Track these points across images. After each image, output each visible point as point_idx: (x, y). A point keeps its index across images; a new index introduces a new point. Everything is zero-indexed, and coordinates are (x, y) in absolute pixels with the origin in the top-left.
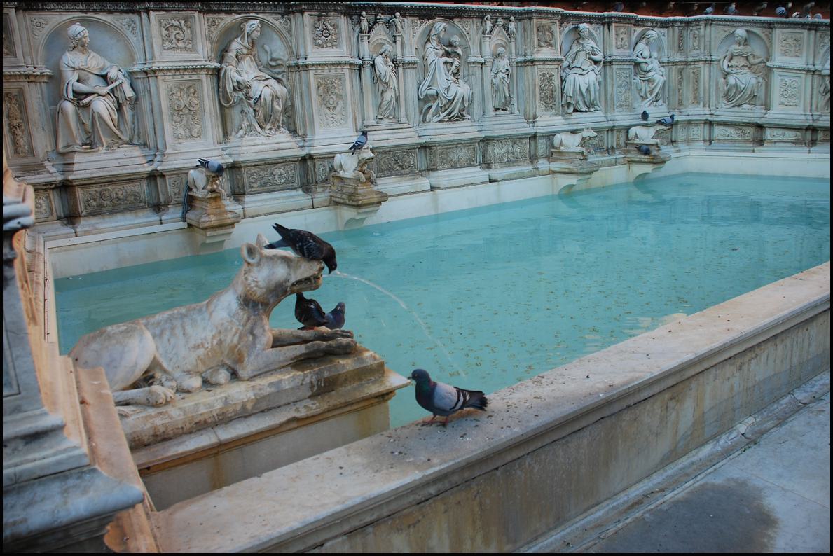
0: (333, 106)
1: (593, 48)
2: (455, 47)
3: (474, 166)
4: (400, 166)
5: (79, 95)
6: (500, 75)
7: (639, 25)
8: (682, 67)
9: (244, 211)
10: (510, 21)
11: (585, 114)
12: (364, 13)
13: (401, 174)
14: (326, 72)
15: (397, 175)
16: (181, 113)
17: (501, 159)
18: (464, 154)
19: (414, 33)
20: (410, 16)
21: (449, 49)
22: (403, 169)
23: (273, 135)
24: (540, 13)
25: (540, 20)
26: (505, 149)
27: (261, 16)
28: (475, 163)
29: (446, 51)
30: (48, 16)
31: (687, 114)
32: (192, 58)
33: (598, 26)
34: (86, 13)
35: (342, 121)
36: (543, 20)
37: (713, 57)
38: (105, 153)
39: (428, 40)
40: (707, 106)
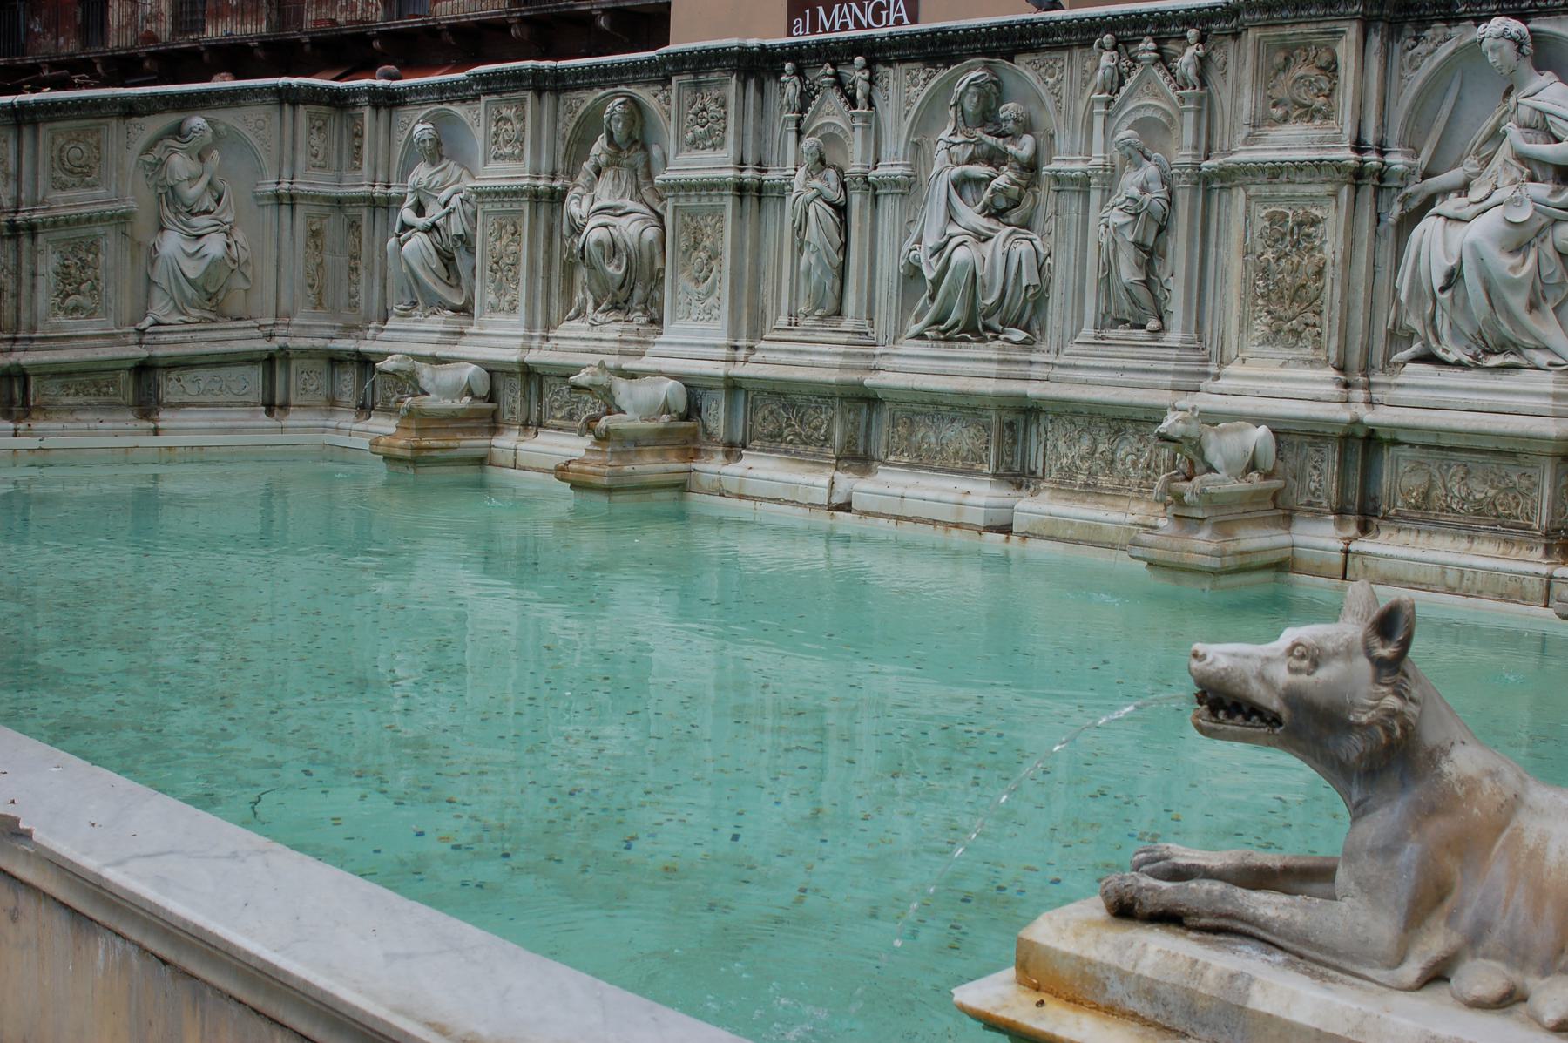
0: (702, 275)
1: (1542, 112)
3: (980, 474)
5: (405, 227)
9: (515, 454)
11: (1445, 371)
12: (788, 66)
13: (797, 453)
14: (694, 202)
15: (786, 453)
16: (495, 266)
17: (1068, 473)
18: (960, 437)
20: (902, 61)
22: (805, 443)
23: (602, 324)
25: (1271, 32)
26: (1085, 445)
27: (633, 90)
28: (986, 469)
30: (413, 112)
32: (516, 172)
34: (441, 103)
35: (715, 312)
36: (1288, 30)
38: (415, 321)
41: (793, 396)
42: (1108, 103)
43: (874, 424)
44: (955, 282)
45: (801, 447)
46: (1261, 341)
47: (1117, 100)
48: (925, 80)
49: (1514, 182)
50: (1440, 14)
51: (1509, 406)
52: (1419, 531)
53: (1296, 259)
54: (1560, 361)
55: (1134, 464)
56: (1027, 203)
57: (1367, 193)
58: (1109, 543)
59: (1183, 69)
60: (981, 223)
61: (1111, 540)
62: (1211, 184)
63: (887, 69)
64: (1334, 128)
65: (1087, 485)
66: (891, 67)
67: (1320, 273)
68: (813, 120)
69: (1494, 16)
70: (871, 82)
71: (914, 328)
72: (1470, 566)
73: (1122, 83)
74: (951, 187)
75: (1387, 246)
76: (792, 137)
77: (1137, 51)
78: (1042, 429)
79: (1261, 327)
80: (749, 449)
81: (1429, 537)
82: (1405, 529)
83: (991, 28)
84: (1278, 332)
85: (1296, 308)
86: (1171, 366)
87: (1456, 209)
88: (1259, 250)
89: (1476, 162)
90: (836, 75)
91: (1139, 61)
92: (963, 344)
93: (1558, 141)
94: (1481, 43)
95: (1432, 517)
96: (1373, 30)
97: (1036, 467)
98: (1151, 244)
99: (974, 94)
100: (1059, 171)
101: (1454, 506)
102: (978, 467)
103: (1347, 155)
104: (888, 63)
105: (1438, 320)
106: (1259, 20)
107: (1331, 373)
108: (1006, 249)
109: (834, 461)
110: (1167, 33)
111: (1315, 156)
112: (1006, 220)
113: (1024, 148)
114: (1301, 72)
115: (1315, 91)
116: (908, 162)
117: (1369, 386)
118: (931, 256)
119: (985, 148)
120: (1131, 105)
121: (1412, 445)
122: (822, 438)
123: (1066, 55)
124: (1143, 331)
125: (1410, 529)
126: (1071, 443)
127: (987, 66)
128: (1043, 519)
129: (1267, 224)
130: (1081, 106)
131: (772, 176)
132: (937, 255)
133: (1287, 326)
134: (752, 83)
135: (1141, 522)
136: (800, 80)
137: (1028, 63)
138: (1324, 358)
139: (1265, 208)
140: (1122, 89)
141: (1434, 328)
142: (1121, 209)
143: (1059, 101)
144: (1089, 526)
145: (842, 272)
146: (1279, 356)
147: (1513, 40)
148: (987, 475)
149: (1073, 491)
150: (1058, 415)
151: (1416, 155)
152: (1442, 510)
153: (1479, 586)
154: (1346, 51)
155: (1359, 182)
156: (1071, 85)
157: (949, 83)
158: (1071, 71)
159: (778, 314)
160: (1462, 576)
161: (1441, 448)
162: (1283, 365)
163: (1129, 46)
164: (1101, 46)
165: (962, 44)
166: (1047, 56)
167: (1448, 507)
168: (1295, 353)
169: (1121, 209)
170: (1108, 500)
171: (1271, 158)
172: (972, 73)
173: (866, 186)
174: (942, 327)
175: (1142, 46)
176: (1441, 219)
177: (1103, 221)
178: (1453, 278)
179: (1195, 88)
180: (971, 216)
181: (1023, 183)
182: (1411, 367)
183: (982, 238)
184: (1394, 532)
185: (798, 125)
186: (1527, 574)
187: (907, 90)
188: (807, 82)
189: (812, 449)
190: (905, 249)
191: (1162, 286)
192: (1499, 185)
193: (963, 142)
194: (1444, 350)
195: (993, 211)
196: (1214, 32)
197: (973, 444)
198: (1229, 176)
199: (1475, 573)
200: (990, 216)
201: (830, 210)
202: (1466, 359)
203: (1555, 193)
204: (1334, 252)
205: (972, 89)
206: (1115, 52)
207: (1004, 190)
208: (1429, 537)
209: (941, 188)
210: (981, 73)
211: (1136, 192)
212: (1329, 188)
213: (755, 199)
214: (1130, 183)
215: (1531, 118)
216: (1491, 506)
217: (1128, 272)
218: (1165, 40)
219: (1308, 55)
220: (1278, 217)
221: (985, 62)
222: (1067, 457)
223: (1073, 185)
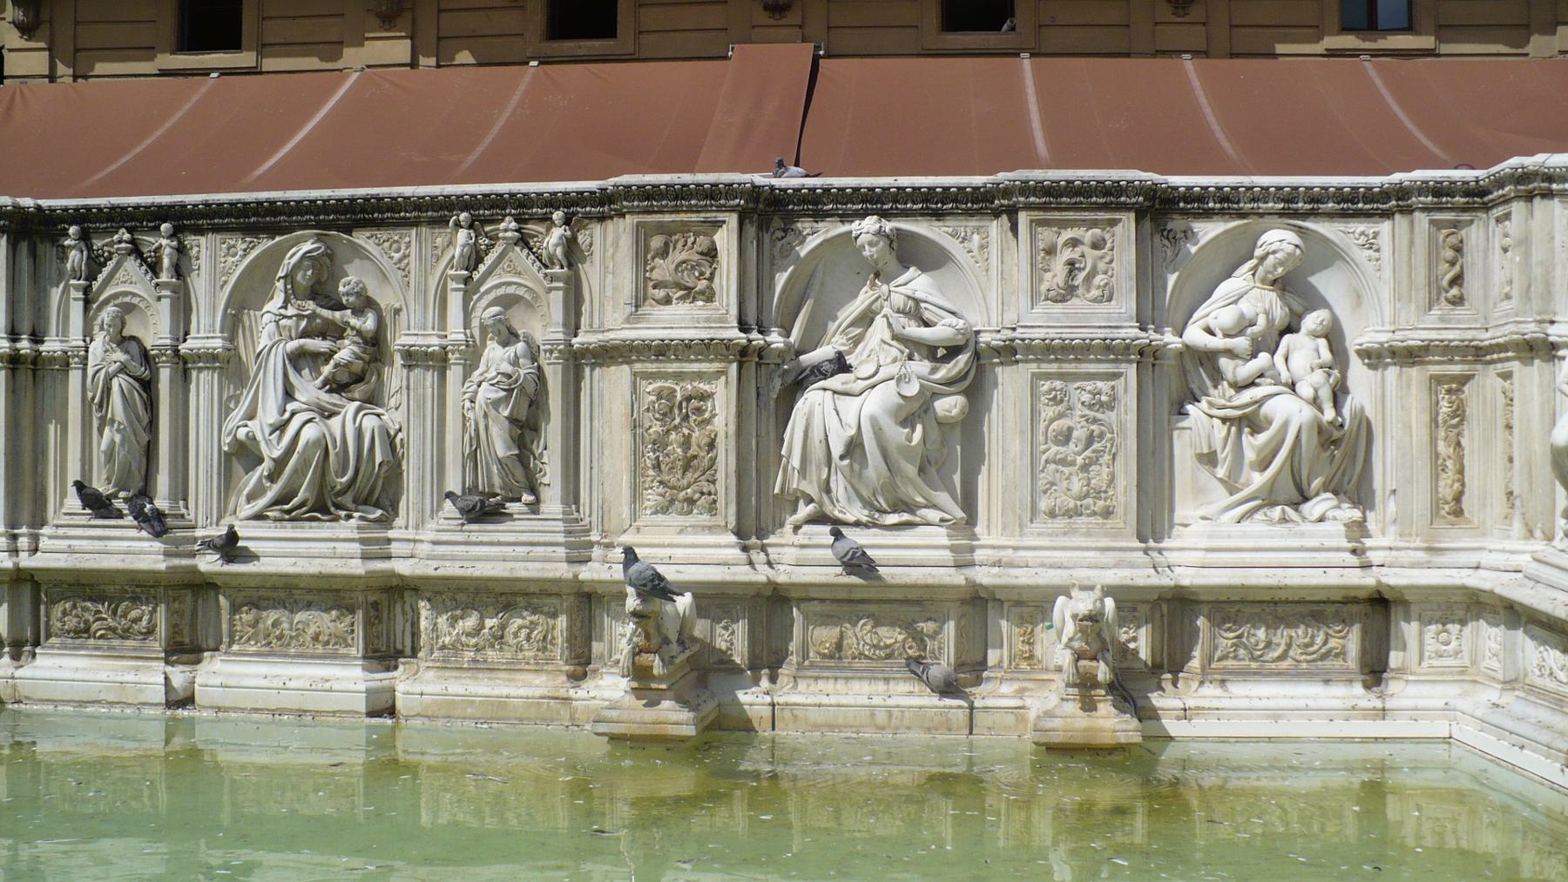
1: (917, 301)
4: (109, 629)
7: (1208, 214)
8: (1456, 369)
12: (72, 230)
15: (97, 648)
17: (456, 647)
18: (320, 621)
20: (216, 229)
24: (649, 194)
26: (470, 622)
29: (325, 320)
31: (1473, 558)
33: (974, 222)
36: (667, 218)
37: (1552, 330)
40: (1538, 533)
41: (102, 587)
42: (467, 280)
43: (200, 613)
45: (116, 642)
46: (653, 509)
48: (245, 250)
49: (895, 360)
50: (808, 209)
51: (902, 559)
52: (836, 678)
53: (686, 431)
54: (949, 517)
55: (528, 638)
57: (751, 368)
58: (516, 719)
59: (551, 249)
61: (518, 715)
62: (578, 362)
64: (718, 310)
65: (475, 661)
66: (202, 235)
67: (711, 445)
68: (105, 288)
69: (869, 215)
70: (181, 250)
71: (248, 509)
72: (898, 706)
73: (480, 260)
74: (287, 362)
75: (768, 417)
77: (498, 229)
78: (408, 608)
79: (652, 497)
80: (43, 648)
81: (846, 683)
82: (823, 678)
83: (328, 201)
84: (672, 501)
85: (690, 476)
86: (561, 538)
87: (843, 384)
88: (647, 425)
89: (844, 341)
90: (133, 241)
91: (498, 239)
92: (314, 524)
93: (927, 324)
94: (856, 238)
95: (846, 665)
96: (747, 221)
97: (404, 646)
98: (524, 419)
100: (414, 346)
101: (867, 653)
102: (343, 651)
103: (734, 333)
104: (200, 231)
105: (833, 485)
106: (638, 206)
107: (733, 539)
109: (163, 655)
110: (528, 214)
111: (705, 335)
112: (350, 395)
113: (369, 323)
114: (684, 256)
115: (697, 274)
117: (763, 548)
118: (271, 434)
121: (822, 600)
122: (145, 630)
123: (414, 232)
124: (518, 504)
125: (828, 678)
126: (453, 621)
127: (319, 238)
128: (437, 700)
129: (654, 398)
130: (433, 282)
131: (51, 346)
132: (278, 432)
133: (682, 495)
134: (24, 247)
135: (550, 694)
136: (87, 246)
137: (369, 238)
138: (723, 524)
139: (650, 383)
140: (481, 266)
141: (828, 491)
142: (492, 385)
143: (406, 276)
144: (493, 704)
145: (150, 451)
146: (676, 524)
147: (888, 236)
148: (356, 658)
149: (461, 668)
150: (437, 593)
151: (788, 335)
152: (854, 658)
153: (907, 722)
154: (726, 239)
155: (744, 359)
157: (275, 256)
159: (63, 495)
160: (890, 715)
161: (851, 601)
162: (681, 532)
165: (290, 215)
166: (437, 231)
167: (860, 654)
168: (690, 520)
169: (492, 385)
170: (502, 675)
171: (661, 337)
172: (305, 244)
173: (176, 360)
174: (286, 507)
175: (502, 226)
176: (829, 393)
177: (467, 395)
178: (854, 447)
179: (562, 268)
180: (309, 389)
181: (367, 357)
182: (806, 528)
184: (811, 682)
186: (951, 708)
187: (223, 260)
189: (129, 643)
190: (229, 425)
191: (535, 459)
192: (882, 363)
193: (295, 316)
194: (840, 512)
195: (334, 386)
197: (336, 627)
198: (608, 354)
199: (903, 712)
200: (330, 391)
201: (136, 385)
202: (864, 519)
203: (934, 371)
204: (726, 425)
205: (306, 263)
206: (471, 231)
207: (348, 365)
208: (846, 683)
209: (276, 362)
210: (315, 246)
211: (508, 368)
212: (716, 366)
213: (30, 372)
214: (496, 356)
215: (905, 305)
216: (901, 649)
217: (500, 444)
218: (526, 221)
219: (686, 241)
220: (665, 393)
221: (317, 235)
222: (450, 634)
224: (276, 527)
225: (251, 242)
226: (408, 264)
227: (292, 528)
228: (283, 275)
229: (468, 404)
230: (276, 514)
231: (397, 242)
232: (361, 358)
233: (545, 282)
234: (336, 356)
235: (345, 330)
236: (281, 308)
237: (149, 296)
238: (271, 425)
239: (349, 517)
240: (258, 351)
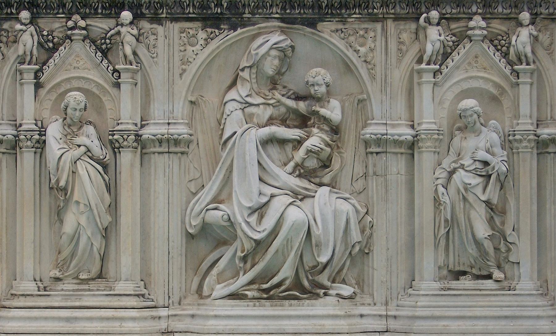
2: (318, 100)
6: (461, 177)
10: (521, 25)
12: (25, 15)
19: (185, 62)
21: (302, 106)
29: (289, 110)
39: (233, 84)
42: (435, 73)
44: (288, 241)
47: (445, 71)
48: (206, 40)
56: (336, 164)
60: (295, 182)
63: (155, 26)
73: (446, 56)
76: (29, 90)
98: (496, 203)
99: (275, 57)
104: (156, 19)
108: (333, 208)
112: (317, 180)
116: (187, 121)
118: (250, 215)
119: (283, 110)
120: (459, 75)
123: (378, 26)
127: (283, 31)
142: (466, 171)
156: (386, 54)
158: (386, 42)
163: (451, 23)
164: (428, 21)
173: (135, 144)
174: (265, 286)
175: (472, 24)
177: (439, 181)
183: (300, 197)
185: (36, 77)
187: (182, 48)
188: (45, 33)
196: (542, 16)
200: (300, 176)
205: (274, 53)
206: (439, 28)
211: (482, 155)
223: (395, 147)
224: (254, 306)
225: (212, 33)
226: (373, 57)
227: (272, 306)
228: (248, 65)
229: (441, 189)
230: (256, 294)
231: (363, 36)
232: (328, 145)
233: (511, 77)
234: (308, 144)
235: (310, 119)
236: (247, 96)
237: (106, 80)
238: (250, 208)
239: (326, 294)
240: (226, 136)
